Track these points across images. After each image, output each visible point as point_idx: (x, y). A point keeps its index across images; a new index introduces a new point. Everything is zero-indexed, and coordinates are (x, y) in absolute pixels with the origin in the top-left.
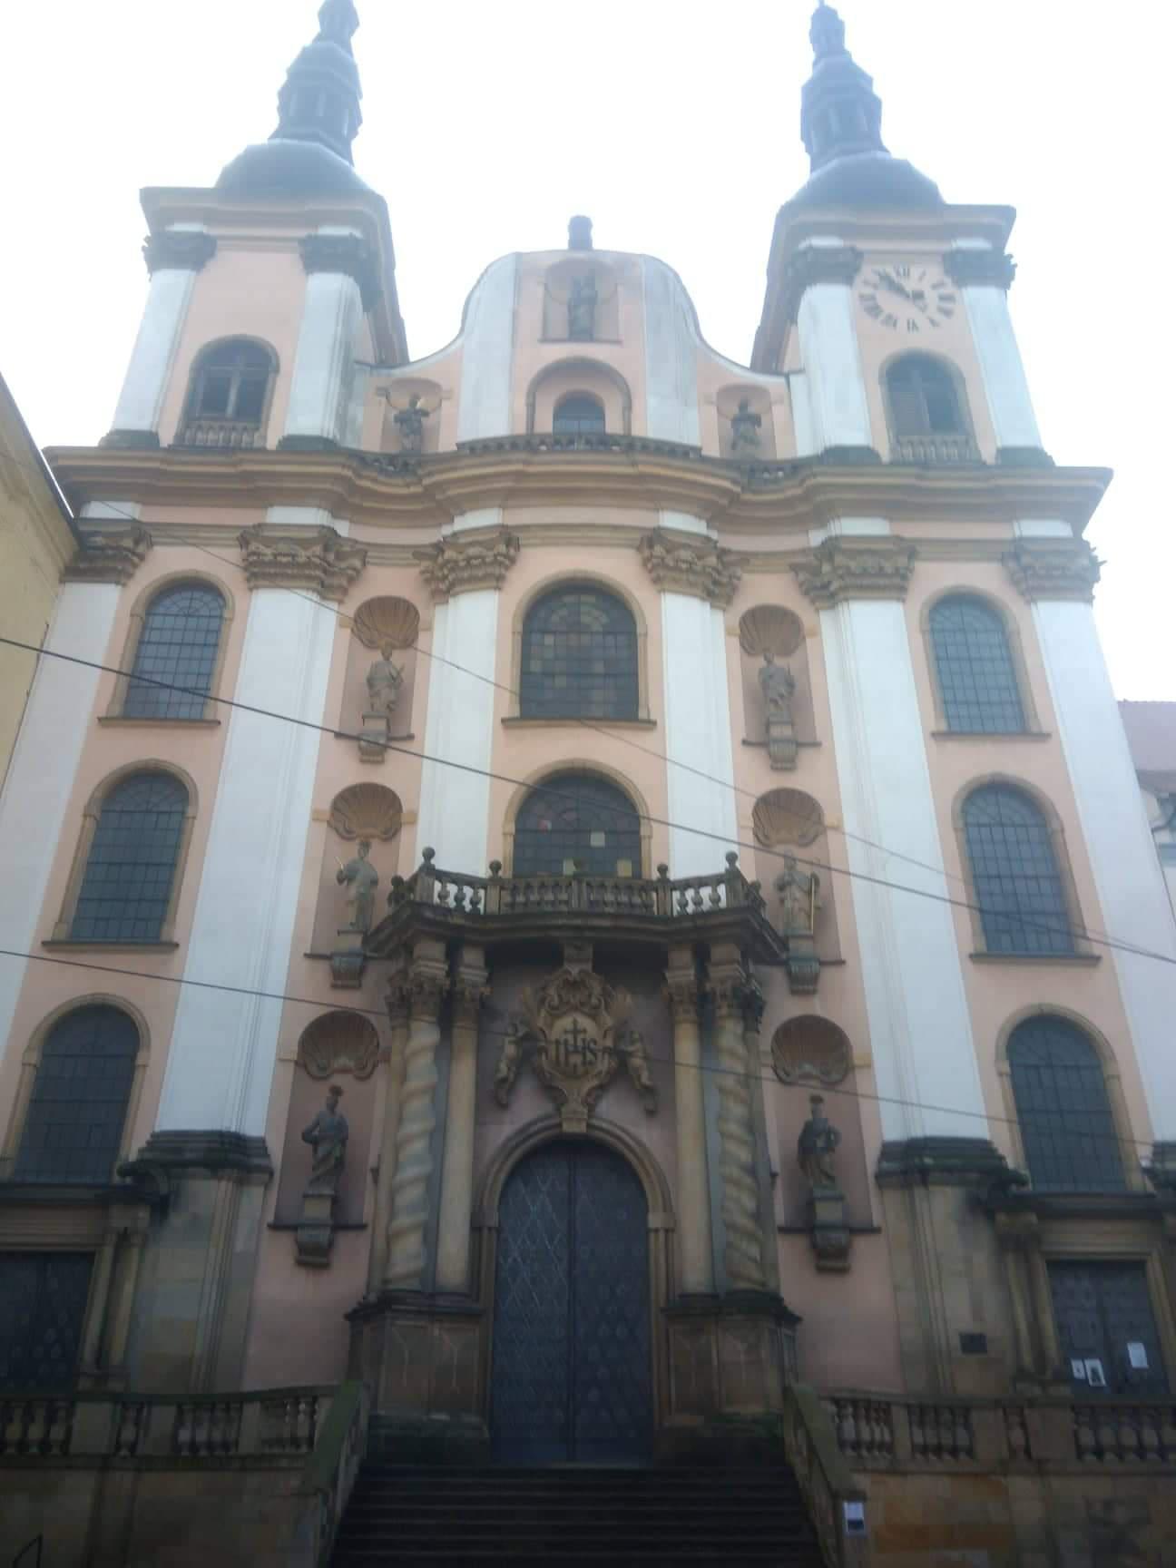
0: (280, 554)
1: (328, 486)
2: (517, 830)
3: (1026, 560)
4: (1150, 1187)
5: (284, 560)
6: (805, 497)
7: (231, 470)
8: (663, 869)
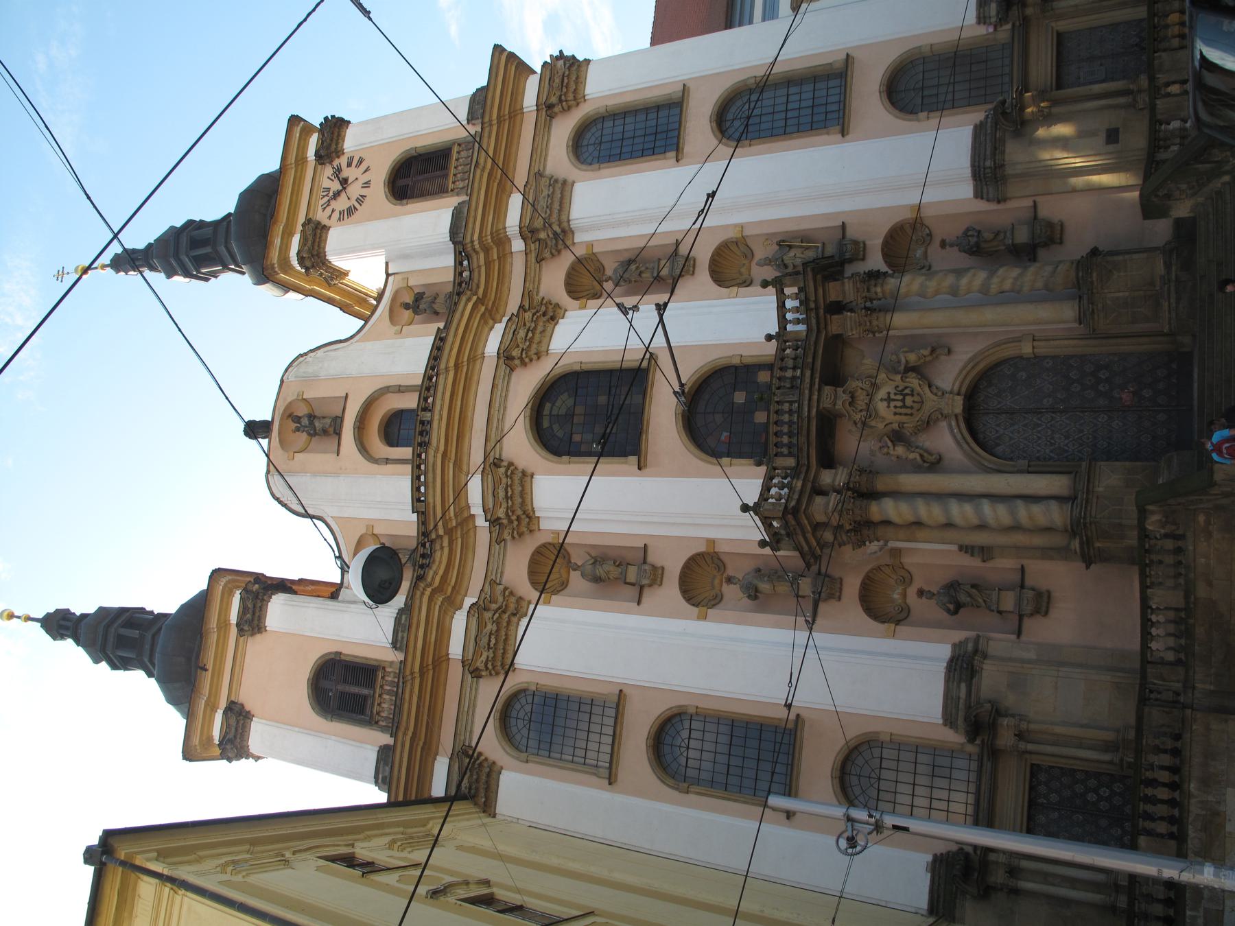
0: (489, 645)
1: (437, 608)
2: (728, 457)
3: (554, 100)
4: (1009, 26)
5: (493, 641)
6: (487, 250)
7: (417, 681)
8: (769, 338)
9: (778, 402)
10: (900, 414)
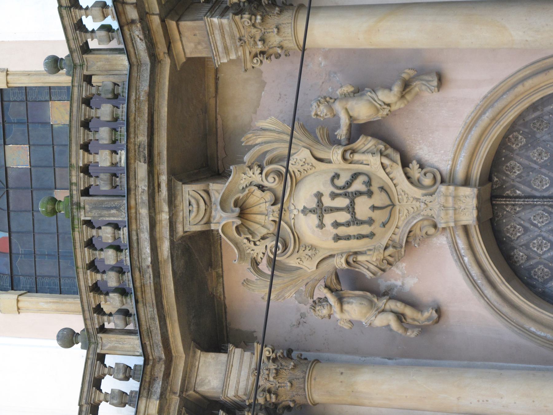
9: (89, 223)
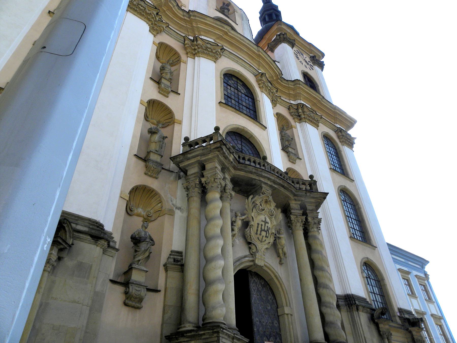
10: (258, 227)
